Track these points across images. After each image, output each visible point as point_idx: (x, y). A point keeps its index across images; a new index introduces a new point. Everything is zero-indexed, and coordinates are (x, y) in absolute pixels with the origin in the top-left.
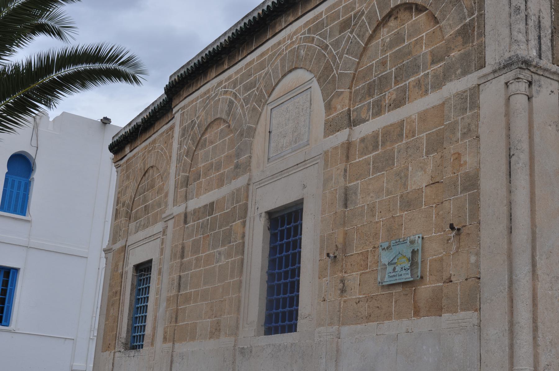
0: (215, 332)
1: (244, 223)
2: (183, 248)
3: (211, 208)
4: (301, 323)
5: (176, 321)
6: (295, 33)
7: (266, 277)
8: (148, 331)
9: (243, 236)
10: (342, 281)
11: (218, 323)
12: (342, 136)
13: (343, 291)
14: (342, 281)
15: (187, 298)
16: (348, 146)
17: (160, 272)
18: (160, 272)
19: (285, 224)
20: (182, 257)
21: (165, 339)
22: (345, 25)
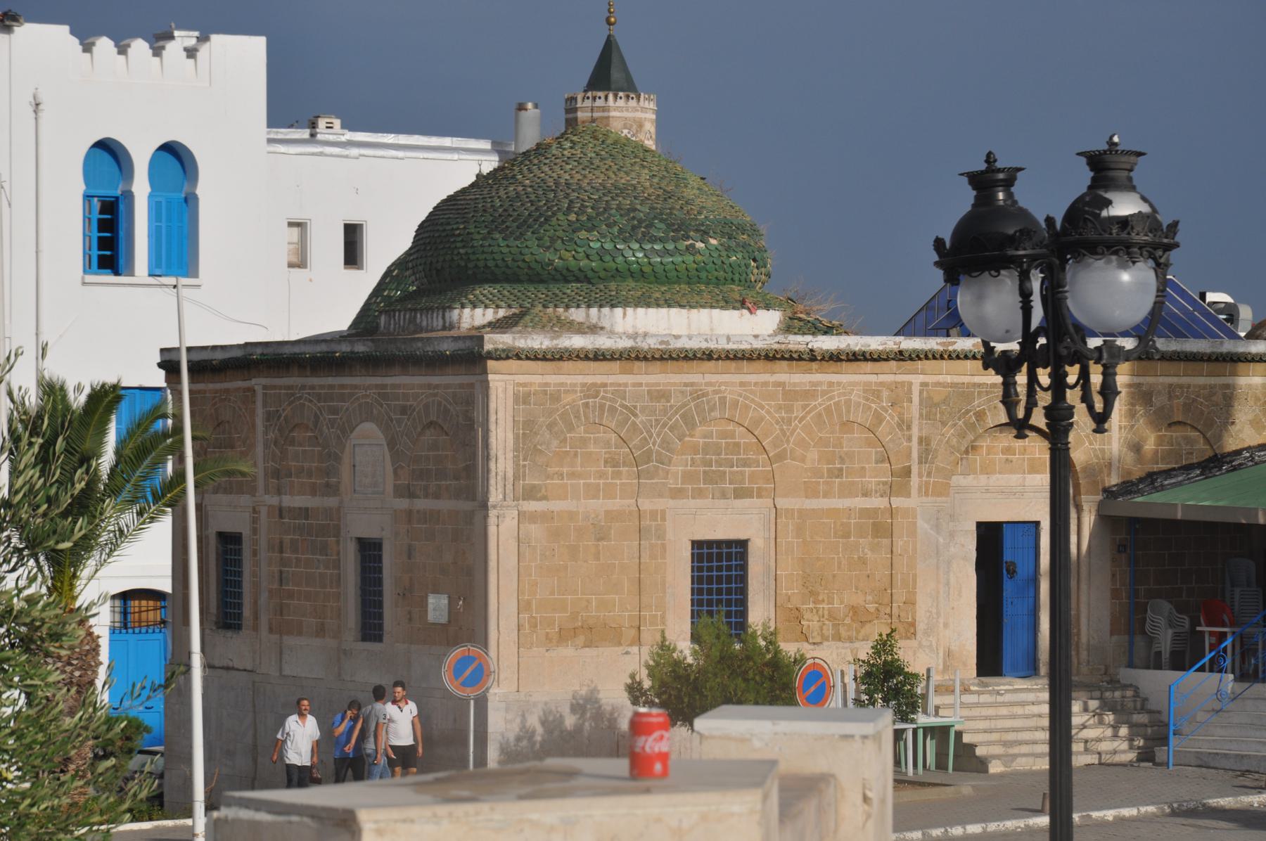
0: (321, 631)
1: (338, 543)
2: (281, 543)
3: (305, 512)
4: (385, 638)
5: (281, 614)
6: (369, 387)
7: (359, 592)
8: (247, 612)
9: (338, 554)
10: (410, 613)
11: (323, 624)
12: (403, 504)
13: (410, 619)
14: (410, 613)
15: (291, 595)
16: (409, 513)
17: (255, 553)
18: (255, 553)
19: (370, 550)
20: (281, 551)
21: (271, 630)
22: (404, 410)
